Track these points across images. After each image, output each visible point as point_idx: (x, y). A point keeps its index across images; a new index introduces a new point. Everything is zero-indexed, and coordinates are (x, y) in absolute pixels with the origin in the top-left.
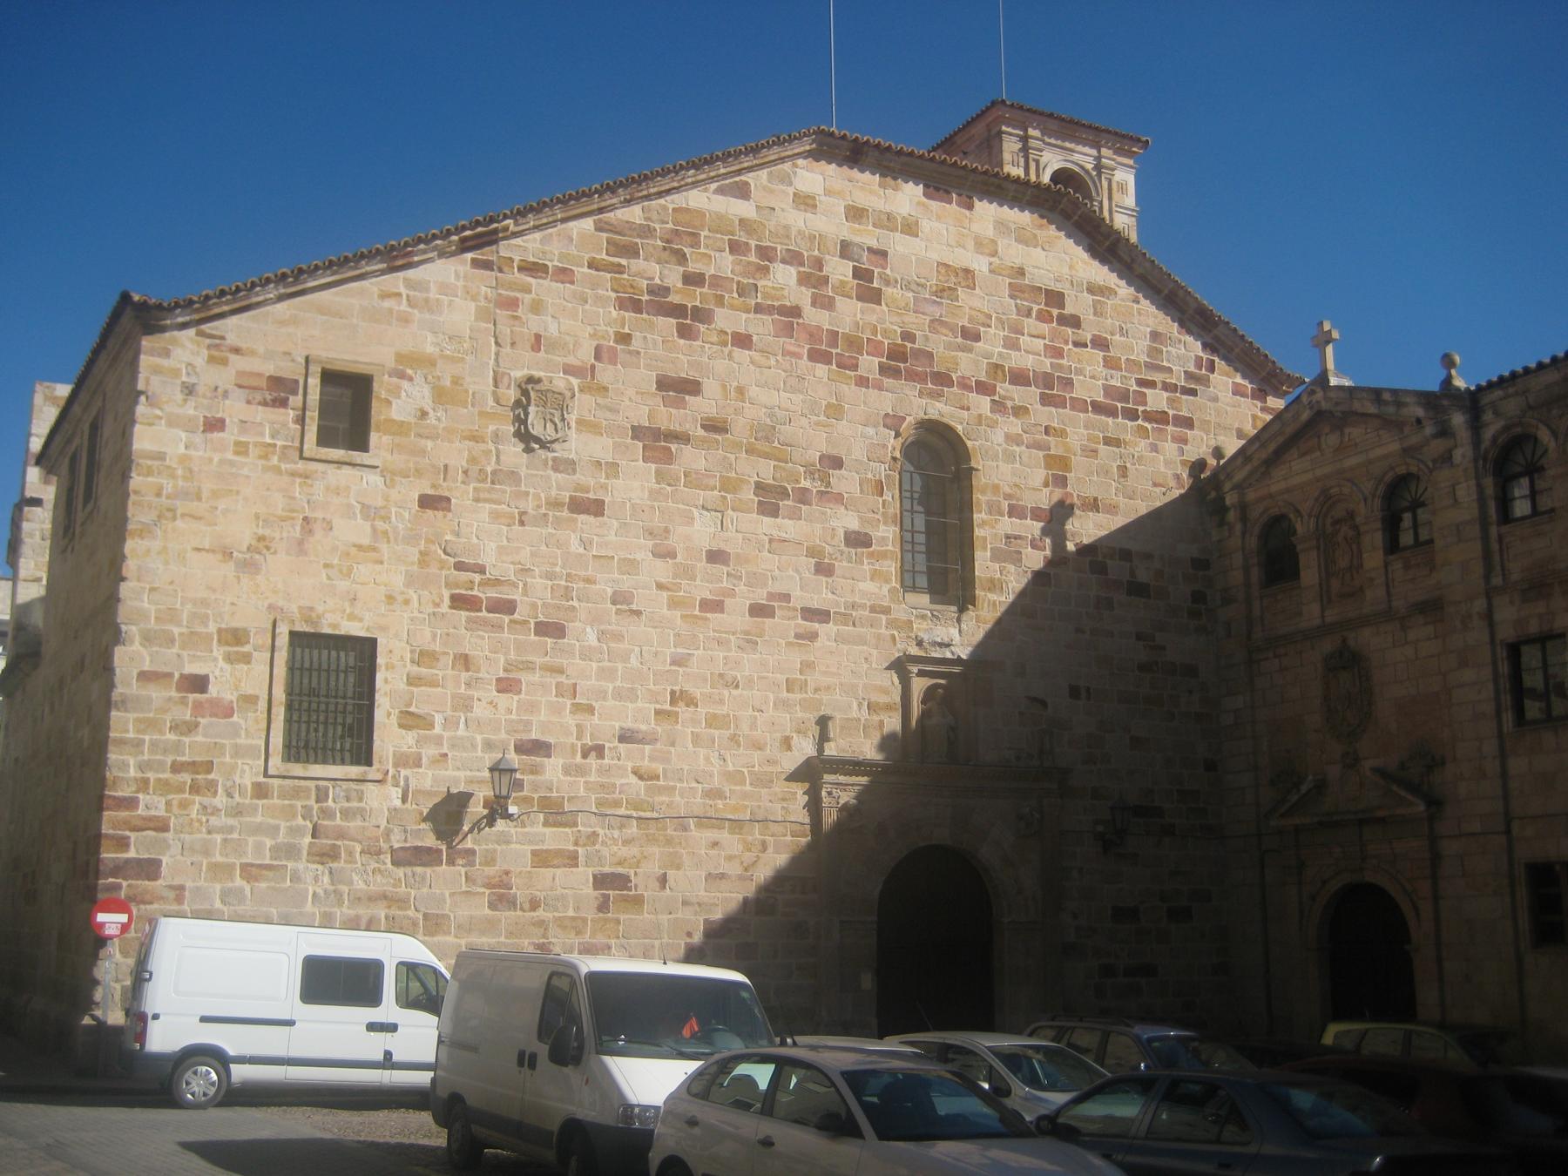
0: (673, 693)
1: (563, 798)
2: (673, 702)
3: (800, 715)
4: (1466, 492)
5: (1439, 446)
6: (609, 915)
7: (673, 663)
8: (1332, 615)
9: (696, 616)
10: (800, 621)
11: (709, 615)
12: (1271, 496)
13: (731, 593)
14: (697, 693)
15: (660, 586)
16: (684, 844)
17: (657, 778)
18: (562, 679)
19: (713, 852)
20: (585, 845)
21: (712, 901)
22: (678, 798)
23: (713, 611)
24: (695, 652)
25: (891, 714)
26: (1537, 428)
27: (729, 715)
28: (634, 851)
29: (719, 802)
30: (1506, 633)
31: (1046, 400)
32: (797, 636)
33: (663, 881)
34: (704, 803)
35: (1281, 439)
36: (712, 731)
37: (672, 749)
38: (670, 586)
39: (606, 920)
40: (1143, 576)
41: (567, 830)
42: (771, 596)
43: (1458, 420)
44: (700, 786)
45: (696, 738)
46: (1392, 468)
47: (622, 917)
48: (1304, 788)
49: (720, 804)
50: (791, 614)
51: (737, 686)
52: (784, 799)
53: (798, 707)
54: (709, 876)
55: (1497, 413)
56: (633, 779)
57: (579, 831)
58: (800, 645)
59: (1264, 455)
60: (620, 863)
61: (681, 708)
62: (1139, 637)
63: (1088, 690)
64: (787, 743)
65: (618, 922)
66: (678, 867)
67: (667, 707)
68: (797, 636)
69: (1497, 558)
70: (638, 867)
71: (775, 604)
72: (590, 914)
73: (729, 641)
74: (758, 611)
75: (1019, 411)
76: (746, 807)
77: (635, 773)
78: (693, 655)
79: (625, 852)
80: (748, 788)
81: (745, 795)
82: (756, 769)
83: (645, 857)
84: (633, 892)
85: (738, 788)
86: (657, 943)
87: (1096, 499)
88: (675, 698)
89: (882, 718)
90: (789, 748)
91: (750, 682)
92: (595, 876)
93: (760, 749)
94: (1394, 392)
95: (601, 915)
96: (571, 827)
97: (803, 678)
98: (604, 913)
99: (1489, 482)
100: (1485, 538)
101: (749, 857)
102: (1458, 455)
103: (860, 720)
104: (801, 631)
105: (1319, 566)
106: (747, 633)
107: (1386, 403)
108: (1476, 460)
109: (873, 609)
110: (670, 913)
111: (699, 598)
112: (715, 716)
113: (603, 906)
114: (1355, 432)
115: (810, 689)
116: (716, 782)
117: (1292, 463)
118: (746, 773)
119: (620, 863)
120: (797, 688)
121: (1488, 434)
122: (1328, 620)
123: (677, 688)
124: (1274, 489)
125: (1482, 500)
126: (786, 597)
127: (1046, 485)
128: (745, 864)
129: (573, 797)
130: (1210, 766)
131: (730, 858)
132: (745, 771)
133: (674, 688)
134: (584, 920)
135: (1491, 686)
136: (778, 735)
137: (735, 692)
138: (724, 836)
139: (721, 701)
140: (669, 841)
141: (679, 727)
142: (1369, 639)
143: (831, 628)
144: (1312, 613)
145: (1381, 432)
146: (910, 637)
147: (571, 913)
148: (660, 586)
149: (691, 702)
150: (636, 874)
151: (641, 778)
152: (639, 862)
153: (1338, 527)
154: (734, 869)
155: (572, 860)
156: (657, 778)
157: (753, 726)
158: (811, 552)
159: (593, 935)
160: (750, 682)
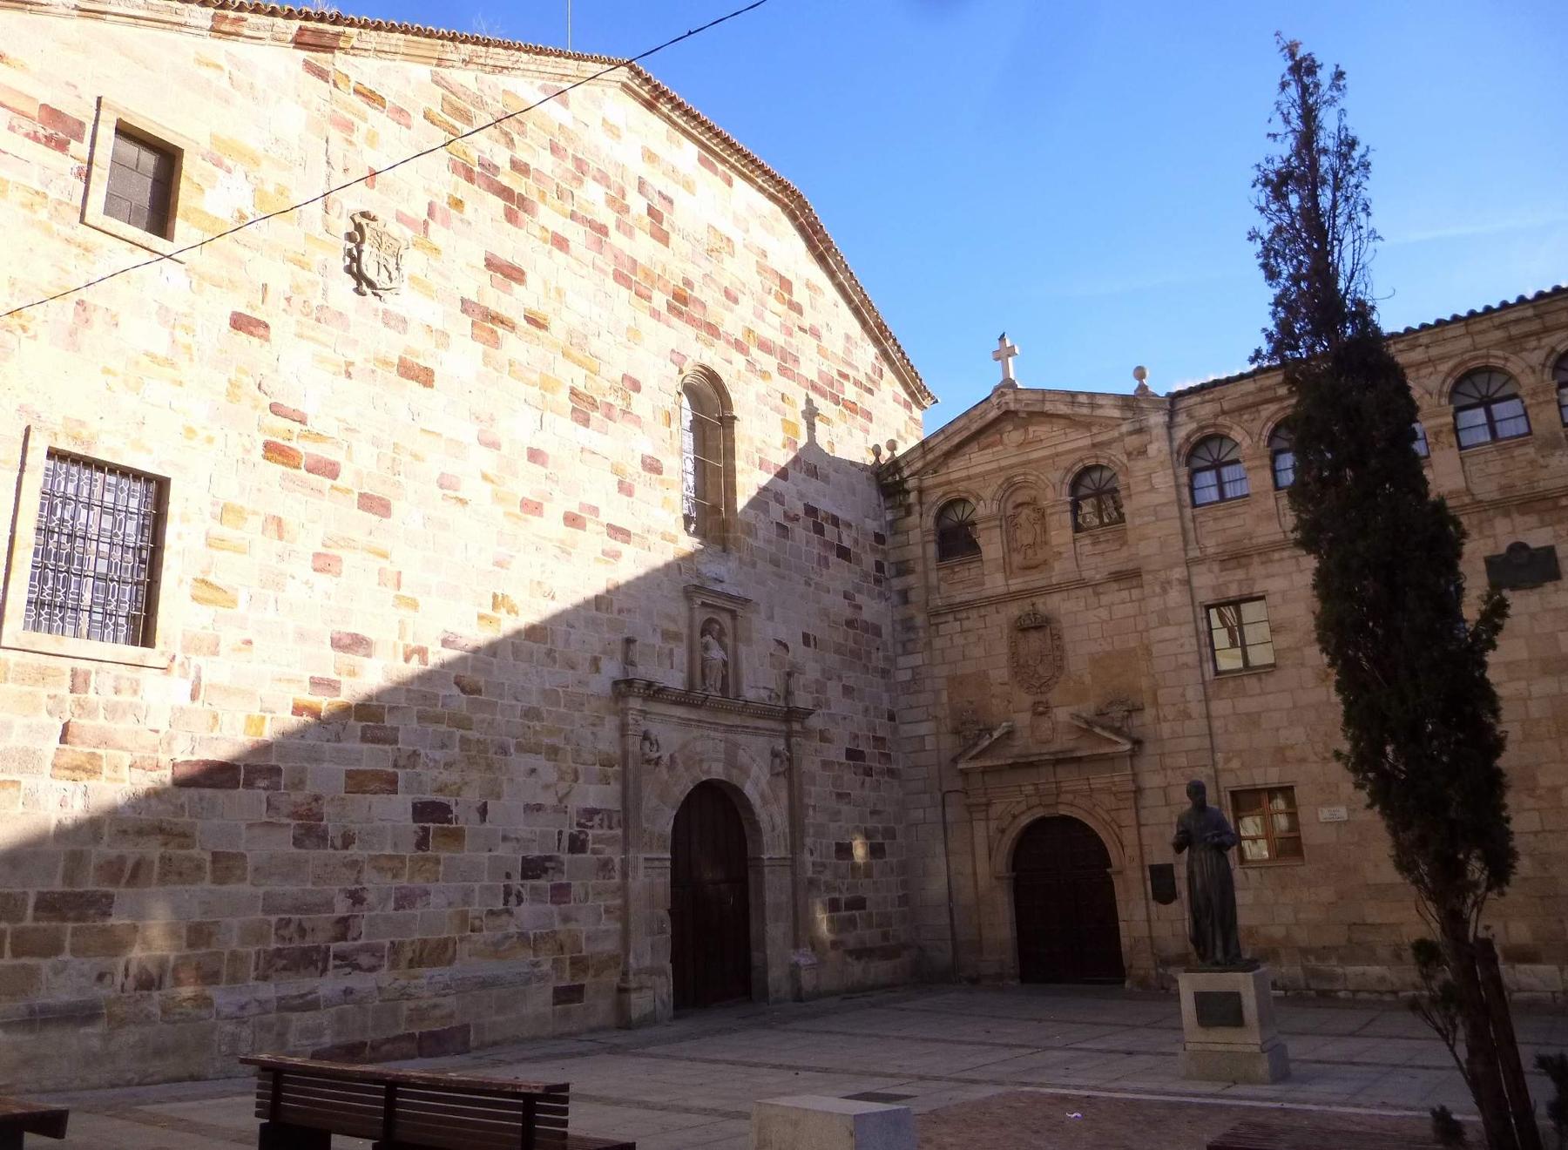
1: (383, 708)
2: (495, 606)
3: (607, 636)
4: (1164, 481)
5: (1133, 442)
6: (429, 852)
8: (1016, 584)
12: (950, 483)
17: (478, 691)
18: (384, 563)
19: (532, 779)
20: (404, 767)
21: (529, 836)
22: (499, 717)
23: (531, 513)
26: (1231, 428)
28: (452, 777)
29: (537, 723)
30: (1206, 596)
31: (783, 371)
33: (483, 811)
34: (522, 724)
35: (965, 434)
37: (494, 660)
39: (427, 859)
40: (847, 543)
41: (387, 747)
42: (583, 506)
43: (1157, 419)
44: (519, 704)
46: (1081, 460)
47: (443, 855)
48: (996, 735)
49: (538, 725)
53: (605, 629)
55: (1191, 417)
56: (456, 691)
57: (399, 749)
58: (607, 562)
59: (945, 447)
60: (440, 790)
62: (846, 596)
65: (437, 861)
68: (604, 553)
69: (1191, 535)
70: (458, 795)
72: (408, 851)
74: (572, 520)
75: (765, 375)
76: (561, 730)
77: (457, 684)
79: (446, 776)
80: (562, 710)
82: (569, 690)
83: (466, 783)
84: (454, 825)
85: (554, 709)
86: (477, 886)
87: (815, 467)
89: (670, 646)
90: (598, 670)
92: (414, 806)
93: (573, 668)
94: (1092, 395)
95: (420, 853)
96: (391, 744)
98: (424, 851)
99: (1183, 471)
100: (1182, 517)
101: (563, 787)
102: (1152, 449)
103: (654, 646)
104: (607, 548)
105: (1002, 542)
106: (562, 542)
107: (1081, 405)
108: (1171, 453)
110: (490, 850)
113: (422, 843)
114: (1038, 430)
115: (616, 607)
116: (534, 700)
117: (972, 456)
119: (440, 790)
121: (1181, 434)
122: (1013, 588)
123: (499, 592)
124: (953, 476)
125: (1178, 486)
126: (595, 510)
127: (784, 446)
129: (394, 707)
130: (892, 718)
131: (546, 787)
132: (560, 690)
134: (402, 859)
135: (1194, 641)
136: (588, 656)
138: (540, 762)
140: (489, 767)
142: (1055, 604)
144: (996, 583)
145: (1068, 430)
146: (692, 569)
147: (388, 851)
150: (457, 804)
151: (463, 690)
152: (460, 788)
153: (1020, 509)
154: (549, 800)
155: (390, 784)
156: (478, 691)
157: (567, 642)
158: (616, 470)
159: (412, 877)
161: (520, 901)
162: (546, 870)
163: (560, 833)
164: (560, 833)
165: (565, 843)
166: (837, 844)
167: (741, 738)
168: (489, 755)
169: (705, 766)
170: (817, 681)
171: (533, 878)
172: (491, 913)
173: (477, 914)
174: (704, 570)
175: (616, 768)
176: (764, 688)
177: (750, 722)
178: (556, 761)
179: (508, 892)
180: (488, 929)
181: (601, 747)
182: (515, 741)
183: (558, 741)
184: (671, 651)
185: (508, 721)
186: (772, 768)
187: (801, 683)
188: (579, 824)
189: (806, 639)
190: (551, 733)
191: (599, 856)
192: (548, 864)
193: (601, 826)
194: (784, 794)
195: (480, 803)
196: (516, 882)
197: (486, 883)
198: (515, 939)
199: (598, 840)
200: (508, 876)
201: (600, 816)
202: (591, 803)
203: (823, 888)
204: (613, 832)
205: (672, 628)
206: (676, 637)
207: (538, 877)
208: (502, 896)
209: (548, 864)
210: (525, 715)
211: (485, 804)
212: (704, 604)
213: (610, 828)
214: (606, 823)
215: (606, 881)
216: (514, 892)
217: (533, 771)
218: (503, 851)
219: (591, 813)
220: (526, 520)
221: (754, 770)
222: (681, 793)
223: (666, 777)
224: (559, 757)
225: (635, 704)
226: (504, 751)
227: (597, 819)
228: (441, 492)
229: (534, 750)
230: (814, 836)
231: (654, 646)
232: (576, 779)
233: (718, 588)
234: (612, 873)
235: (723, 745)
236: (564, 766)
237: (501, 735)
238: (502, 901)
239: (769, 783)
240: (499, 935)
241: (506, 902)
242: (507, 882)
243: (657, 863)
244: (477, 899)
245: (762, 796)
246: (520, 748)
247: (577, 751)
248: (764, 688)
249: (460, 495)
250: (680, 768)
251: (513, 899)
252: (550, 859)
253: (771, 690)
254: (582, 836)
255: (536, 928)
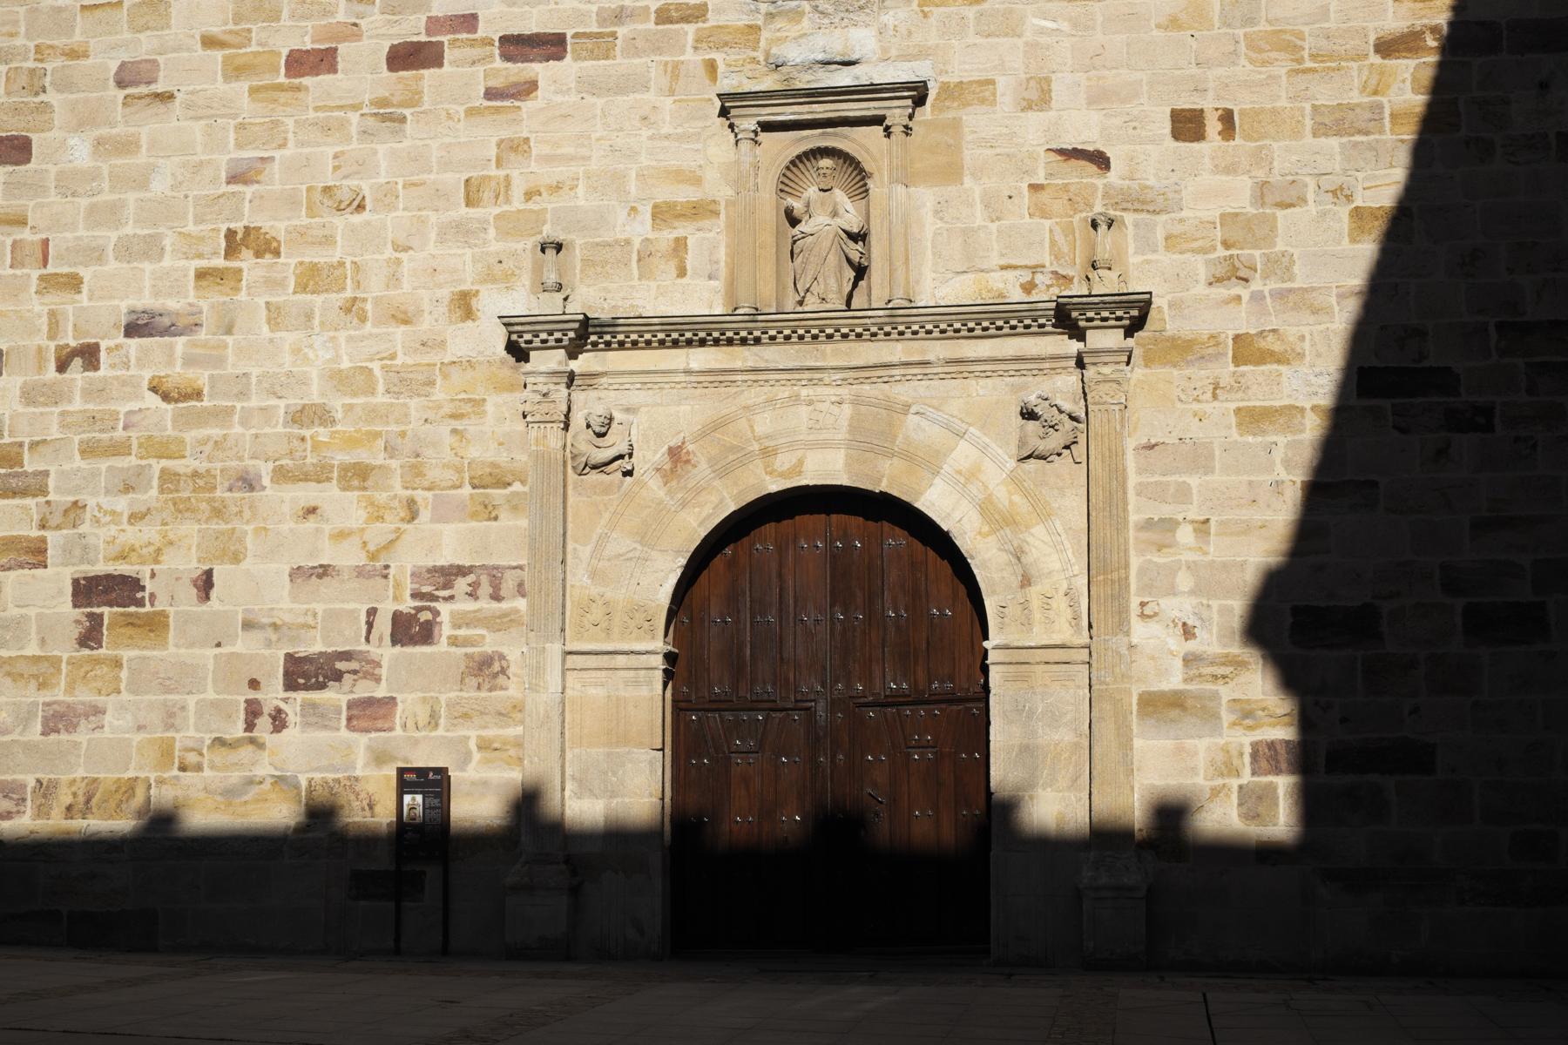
0: (231, 234)
1: (21, 445)
3: (495, 247)
6: (101, 651)
7: (232, 179)
9: (280, 88)
10: (499, 63)
11: (307, 81)
13: (353, 31)
14: (276, 226)
15: (209, 42)
16: (247, 514)
17: (198, 395)
18: (25, 235)
19: (311, 524)
20: (58, 527)
21: (301, 620)
22: (238, 429)
23: (315, 70)
24: (277, 154)
25: (700, 224)
27: (341, 264)
28: (149, 533)
29: (321, 430)
32: (490, 94)
33: (205, 584)
34: (289, 437)
36: (309, 297)
37: (229, 339)
38: (227, 38)
39: (98, 661)
41: (30, 502)
44: (282, 403)
45: (275, 316)
47: (127, 654)
49: (322, 433)
50: (477, 52)
51: (361, 207)
52: (454, 416)
53: (492, 232)
54: (297, 573)
56: (154, 401)
57: (48, 502)
58: (497, 110)
60: (122, 557)
61: (246, 262)
63: (1227, 118)
64: (464, 306)
65: (117, 663)
66: (236, 558)
67: (219, 262)
70: (157, 562)
71: (445, 39)
72: (66, 650)
73: (343, 124)
74: (407, 57)
76: (377, 435)
77: (154, 389)
78: (272, 159)
79: (133, 535)
80: (381, 398)
81: (373, 413)
82: (398, 362)
83: (171, 543)
84: (148, 608)
85: (360, 400)
86: (191, 701)
88: (233, 243)
89: (679, 233)
91: (388, 196)
92: (76, 582)
93: (406, 322)
95: (86, 652)
96: (35, 496)
97: (502, 173)
98: (92, 648)
101: (378, 534)
103: (628, 242)
109: (663, 16)
110: (219, 645)
111: (285, 52)
112: (314, 269)
113: (90, 636)
116: (315, 394)
118: (378, 372)
119: (122, 557)
120: (487, 195)
123: (238, 226)
126: (469, 22)
128: (372, 547)
129: (38, 443)
131: (341, 535)
132: (376, 367)
133: (232, 226)
134: (55, 662)
136: (445, 293)
137: (357, 219)
138: (329, 495)
139: (328, 241)
140: (218, 512)
141: (242, 296)
143: (568, 68)
146: (754, 60)
147: (33, 650)
148: (209, 42)
149: (266, 247)
150: (153, 575)
151: (166, 397)
152: (159, 551)
154: (348, 557)
155: (36, 554)
156: (198, 395)
157: (394, 279)
159: (71, 688)
160: (388, 196)
161: (279, 721)
162: (338, 676)
163: (372, 612)
164: (372, 612)
165: (384, 626)
166: (1295, 611)
167: (901, 392)
168: (218, 493)
169: (784, 461)
170: (1227, 219)
171: (307, 688)
172: (220, 742)
173: (191, 744)
174: (794, 54)
175: (517, 487)
176: (1003, 268)
177: (938, 350)
178: (365, 489)
179: (253, 712)
180: (212, 767)
181: (474, 452)
182: (270, 465)
183: (374, 456)
184: (680, 245)
185: (257, 436)
186: (1022, 443)
187: (1160, 234)
188: (415, 595)
189: (1187, 125)
190: (351, 442)
191: (470, 650)
192: (341, 665)
193: (472, 595)
194: (1072, 507)
195: (199, 572)
196: (273, 694)
197: (211, 695)
198: (267, 786)
199: (460, 621)
200: (254, 684)
201: (471, 578)
202: (445, 559)
203: (1226, 717)
204: (504, 605)
205: (684, 194)
206: (700, 211)
207: (321, 686)
208: (242, 716)
209: (341, 665)
210: (294, 421)
211: (209, 574)
212: (767, 127)
213: (496, 597)
214: (485, 589)
215: (483, 694)
216: (266, 710)
217: (312, 511)
218: (242, 644)
219: (448, 575)
220: (298, 89)
221: (963, 454)
222: (700, 525)
223: (661, 493)
224: (369, 483)
225: (547, 361)
226: (248, 483)
227: (462, 584)
228: (121, 94)
229: (320, 475)
230: (1192, 592)
231: (628, 242)
232: (413, 515)
233: (843, 78)
234: (501, 680)
235: (847, 409)
236: (381, 497)
237: (241, 459)
238: (241, 725)
239: (1014, 480)
240: (235, 777)
241: (250, 726)
242: (252, 695)
243: (621, 660)
244: (192, 721)
245: (987, 508)
246: (281, 475)
247: (413, 466)
248: (1003, 268)
249: (159, 87)
250: (702, 470)
251: (264, 722)
252: (346, 656)
253: (1035, 269)
254: (425, 616)
255: (318, 769)
